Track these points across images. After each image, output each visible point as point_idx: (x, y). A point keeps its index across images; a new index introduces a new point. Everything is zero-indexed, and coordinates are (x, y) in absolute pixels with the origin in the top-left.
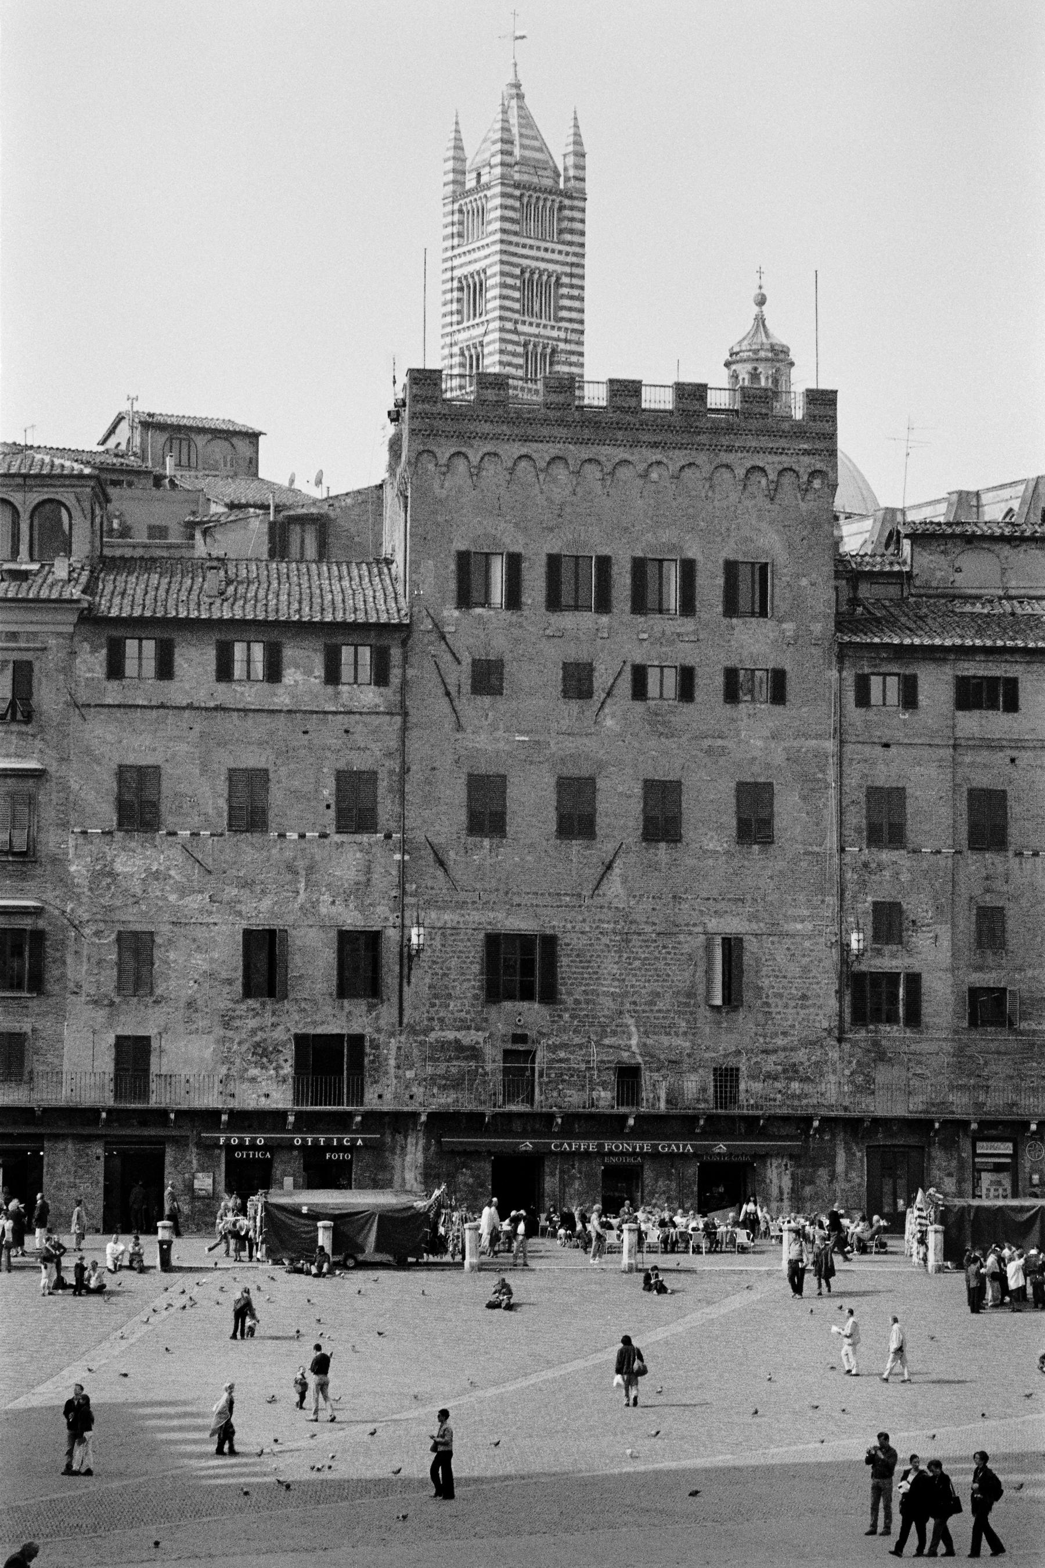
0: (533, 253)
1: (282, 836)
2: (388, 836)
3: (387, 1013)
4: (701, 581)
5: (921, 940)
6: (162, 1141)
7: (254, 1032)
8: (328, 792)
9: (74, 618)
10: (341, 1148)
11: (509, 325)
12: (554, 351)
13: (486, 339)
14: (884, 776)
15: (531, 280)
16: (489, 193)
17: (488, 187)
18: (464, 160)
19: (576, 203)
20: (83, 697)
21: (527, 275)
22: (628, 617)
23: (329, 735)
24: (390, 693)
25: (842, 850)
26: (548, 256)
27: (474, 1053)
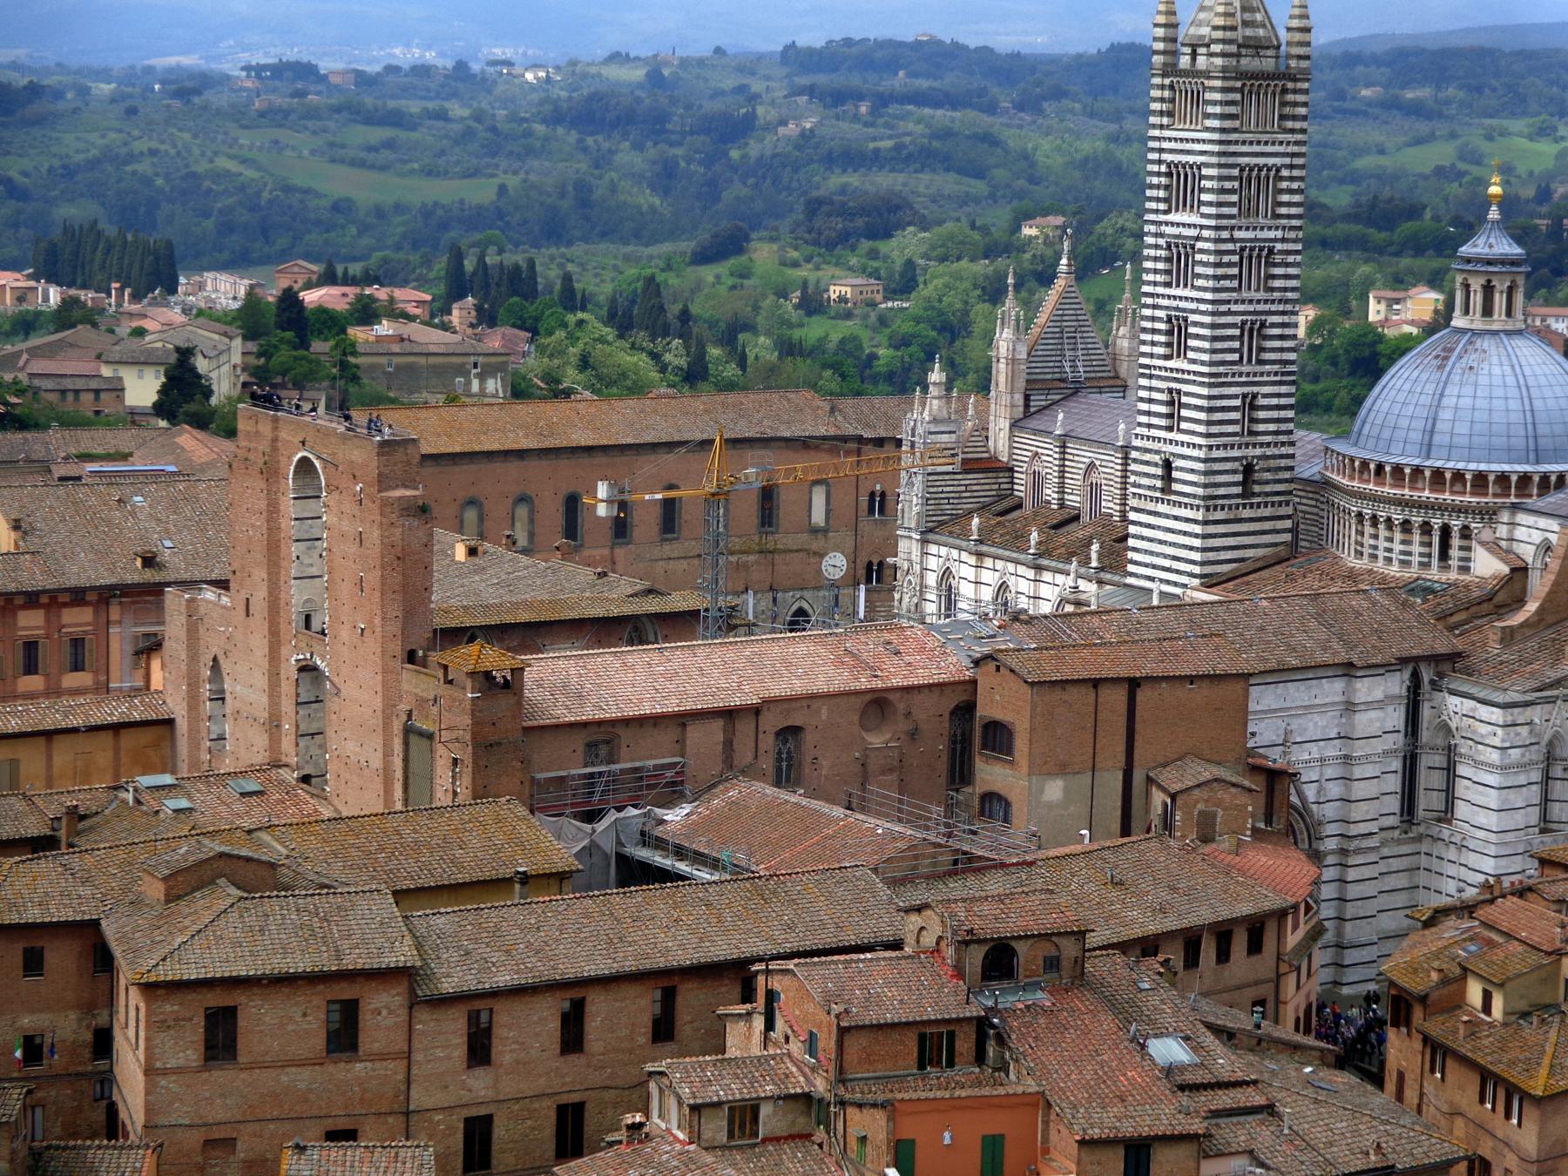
12: (1271, 251)
21: (1245, 174)
26: (1269, 149)
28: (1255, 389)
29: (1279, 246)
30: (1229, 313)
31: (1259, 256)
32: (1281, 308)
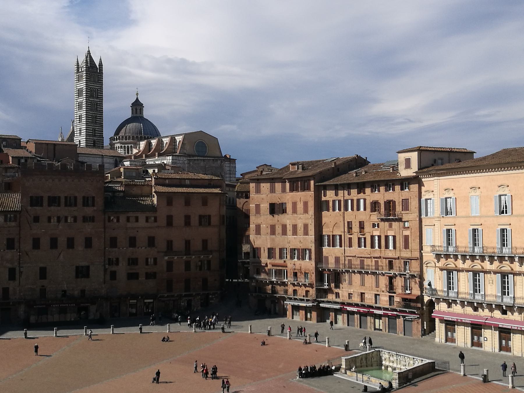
0: (93, 85)
3: (17, 282)
11: (87, 99)
12: (97, 104)
13: (83, 101)
15: (92, 90)
16: (83, 73)
17: (83, 71)
18: (79, 65)
19: (101, 75)
25: (105, 248)
26: (95, 85)
28: (95, 127)
29: (98, 103)
30: (89, 113)
31: (95, 104)
32: (100, 113)
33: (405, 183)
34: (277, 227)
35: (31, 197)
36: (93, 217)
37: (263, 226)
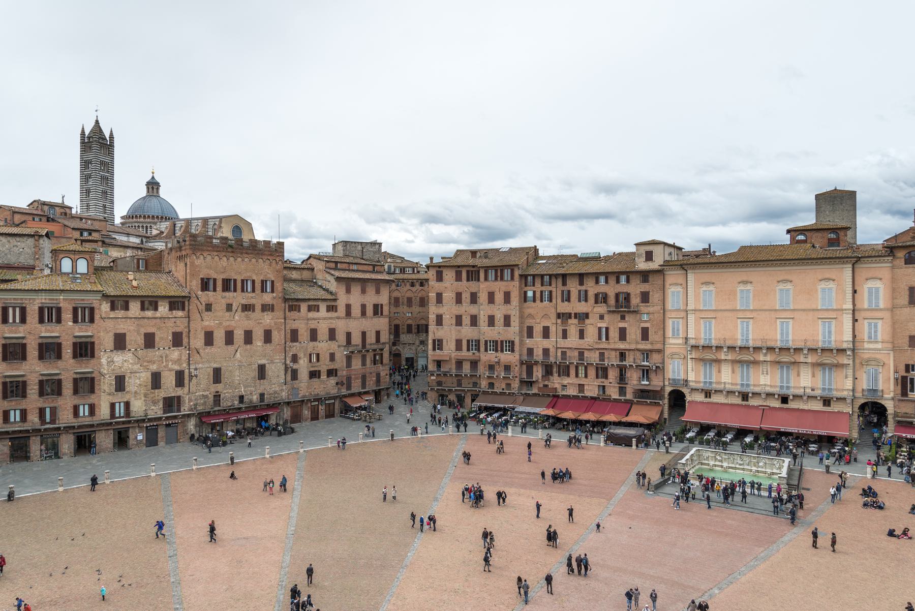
1: (159, 349)
2: (186, 347)
3: (186, 389)
4: (256, 285)
5: (301, 362)
6: (129, 427)
7: (153, 398)
8: (170, 338)
9: (101, 295)
10: (175, 423)
12: (108, 178)
14: (294, 327)
20: (104, 316)
22: (240, 293)
23: (170, 324)
24: (186, 312)
25: (285, 343)
27: (206, 397)
33: (645, 276)
34: (464, 317)
35: (202, 279)
36: (273, 305)
37: (446, 318)
